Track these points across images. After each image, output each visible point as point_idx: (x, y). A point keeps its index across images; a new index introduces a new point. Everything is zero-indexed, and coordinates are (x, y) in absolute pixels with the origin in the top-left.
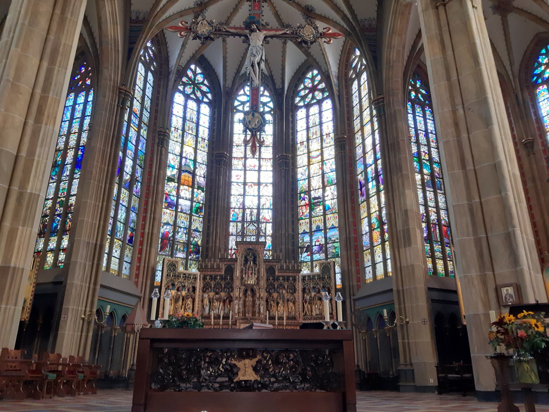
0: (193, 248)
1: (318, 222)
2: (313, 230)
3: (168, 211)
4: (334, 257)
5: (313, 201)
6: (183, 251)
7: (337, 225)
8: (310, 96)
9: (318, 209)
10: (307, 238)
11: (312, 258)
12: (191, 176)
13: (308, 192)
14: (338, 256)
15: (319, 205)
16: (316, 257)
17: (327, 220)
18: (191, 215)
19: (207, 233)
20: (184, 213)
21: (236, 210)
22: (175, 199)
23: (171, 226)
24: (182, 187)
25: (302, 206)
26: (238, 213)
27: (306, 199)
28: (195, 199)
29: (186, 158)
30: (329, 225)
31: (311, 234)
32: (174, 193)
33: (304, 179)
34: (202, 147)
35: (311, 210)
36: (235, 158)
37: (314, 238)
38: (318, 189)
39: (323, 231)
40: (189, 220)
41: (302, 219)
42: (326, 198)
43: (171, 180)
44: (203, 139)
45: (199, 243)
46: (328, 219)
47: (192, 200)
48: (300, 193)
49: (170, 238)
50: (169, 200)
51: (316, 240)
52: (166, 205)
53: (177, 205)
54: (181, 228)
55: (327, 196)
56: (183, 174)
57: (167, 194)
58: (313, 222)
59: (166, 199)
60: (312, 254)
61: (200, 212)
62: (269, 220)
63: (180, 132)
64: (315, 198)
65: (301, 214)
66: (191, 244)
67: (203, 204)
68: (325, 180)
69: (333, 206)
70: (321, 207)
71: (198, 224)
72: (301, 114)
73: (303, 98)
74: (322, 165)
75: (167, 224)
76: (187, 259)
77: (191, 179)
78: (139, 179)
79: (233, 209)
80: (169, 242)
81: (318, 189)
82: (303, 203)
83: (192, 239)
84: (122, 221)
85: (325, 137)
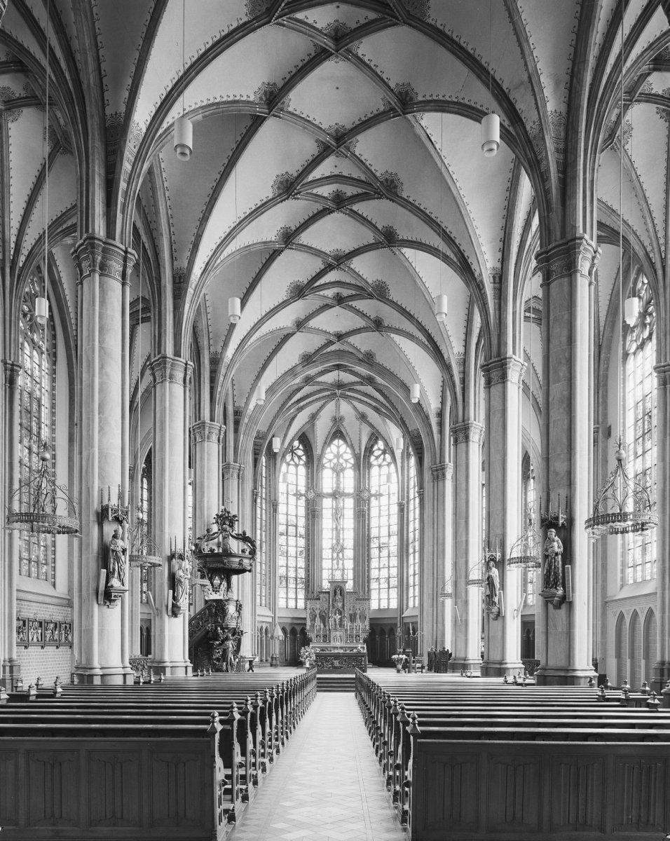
1: (384, 561)
5: (381, 545)
8: (382, 456)
13: (379, 538)
18: (296, 557)
19: (307, 570)
24: (289, 538)
30: (391, 565)
37: (381, 572)
43: (282, 534)
63: (285, 495)
68: (391, 530)
70: (387, 551)
71: (302, 563)
72: (374, 471)
73: (377, 458)
77: (294, 531)
82: (375, 546)
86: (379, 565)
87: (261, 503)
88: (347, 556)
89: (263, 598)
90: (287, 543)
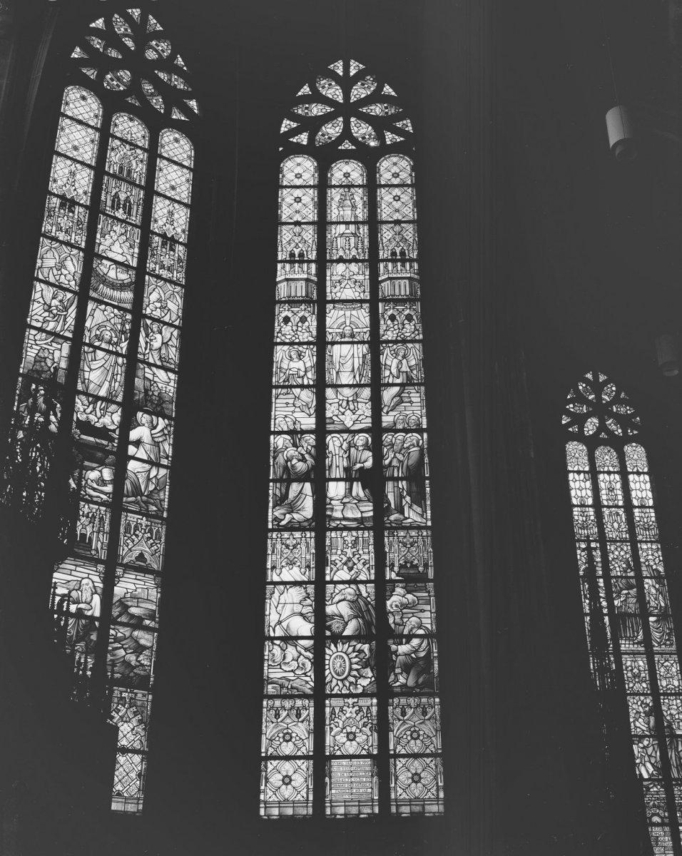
9: (93, 475)
17: (122, 530)
30: (129, 551)
64: (86, 427)
68: (139, 383)
69: (151, 487)
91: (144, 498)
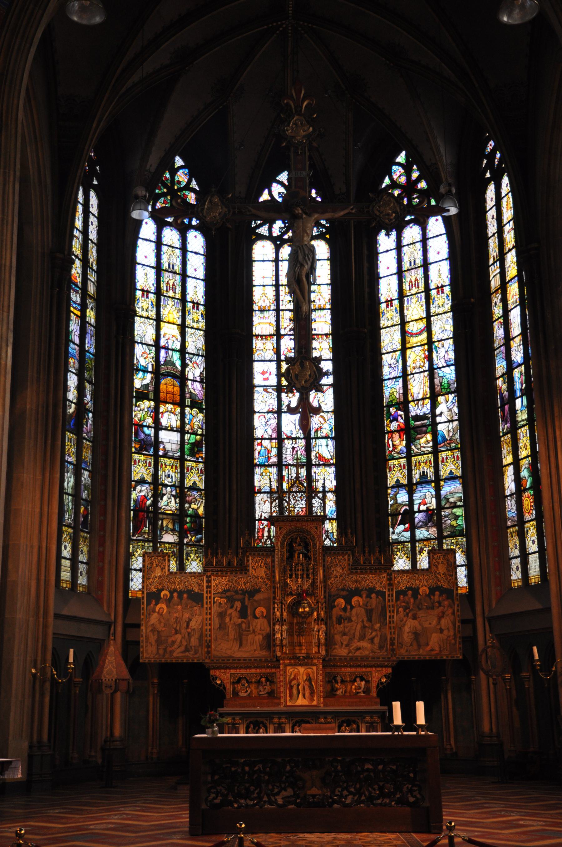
0: (190, 522)
2: (414, 481)
3: (142, 458)
4: (453, 535)
6: (173, 530)
7: (458, 473)
9: (423, 440)
10: (403, 497)
11: (413, 535)
12: (177, 383)
14: (461, 534)
15: (426, 433)
16: (421, 533)
17: (440, 462)
20: (169, 458)
21: (266, 443)
22: (150, 432)
23: (147, 486)
24: (162, 409)
25: (392, 432)
26: (269, 447)
27: (399, 418)
28: (187, 428)
29: (166, 348)
30: (444, 472)
31: (411, 488)
32: (150, 421)
33: (396, 378)
34: (194, 321)
35: (410, 442)
36: (257, 336)
37: (416, 496)
38: (423, 399)
39: (433, 484)
40: (179, 470)
41: (393, 458)
42: (438, 419)
43: (142, 395)
44: (196, 305)
45: (201, 511)
46: (443, 461)
47: (182, 430)
48: (389, 406)
49: (148, 507)
50: (142, 436)
51: (420, 501)
52: (137, 446)
53: (157, 442)
54: (166, 486)
55: (441, 414)
56: (163, 381)
57: (137, 425)
58: (413, 464)
59: (137, 434)
60: (412, 529)
61: (200, 451)
62: (329, 460)
63: (152, 297)
64: (417, 418)
65: (391, 449)
66: (188, 516)
67: (201, 435)
68: (437, 381)
69: (451, 434)
70: (429, 437)
74: (430, 351)
75: (142, 481)
76: (180, 544)
77: (177, 390)
78: (90, 406)
79: (259, 441)
80: (148, 517)
81: (423, 399)
82: (394, 426)
83: (187, 505)
84: (70, 491)
85: (433, 293)
86: (410, 476)
87: (83, 307)
88: (320, 457)
89: (82, 568)
90: (157, 421)
91: (448, 442)
